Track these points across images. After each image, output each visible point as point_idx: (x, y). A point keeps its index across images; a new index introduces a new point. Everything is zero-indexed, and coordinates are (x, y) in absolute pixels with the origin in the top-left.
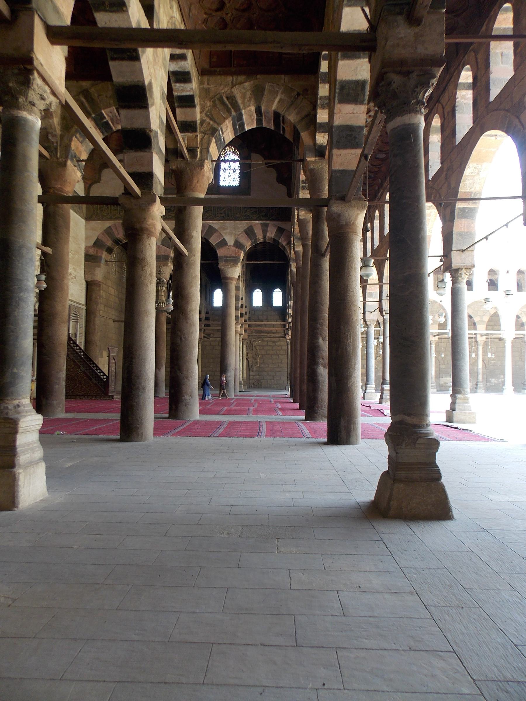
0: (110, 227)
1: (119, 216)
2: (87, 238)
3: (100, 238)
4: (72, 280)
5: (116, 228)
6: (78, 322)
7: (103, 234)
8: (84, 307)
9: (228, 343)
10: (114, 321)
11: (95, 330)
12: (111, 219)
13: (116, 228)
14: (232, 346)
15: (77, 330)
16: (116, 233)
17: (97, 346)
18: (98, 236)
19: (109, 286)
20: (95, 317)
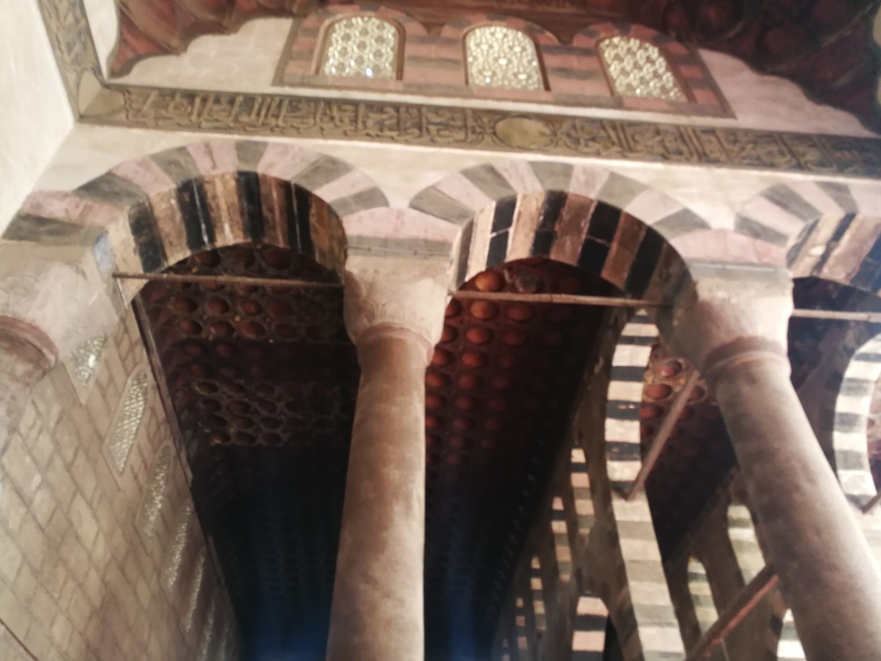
1: (232, 125)
2: (56, 168)
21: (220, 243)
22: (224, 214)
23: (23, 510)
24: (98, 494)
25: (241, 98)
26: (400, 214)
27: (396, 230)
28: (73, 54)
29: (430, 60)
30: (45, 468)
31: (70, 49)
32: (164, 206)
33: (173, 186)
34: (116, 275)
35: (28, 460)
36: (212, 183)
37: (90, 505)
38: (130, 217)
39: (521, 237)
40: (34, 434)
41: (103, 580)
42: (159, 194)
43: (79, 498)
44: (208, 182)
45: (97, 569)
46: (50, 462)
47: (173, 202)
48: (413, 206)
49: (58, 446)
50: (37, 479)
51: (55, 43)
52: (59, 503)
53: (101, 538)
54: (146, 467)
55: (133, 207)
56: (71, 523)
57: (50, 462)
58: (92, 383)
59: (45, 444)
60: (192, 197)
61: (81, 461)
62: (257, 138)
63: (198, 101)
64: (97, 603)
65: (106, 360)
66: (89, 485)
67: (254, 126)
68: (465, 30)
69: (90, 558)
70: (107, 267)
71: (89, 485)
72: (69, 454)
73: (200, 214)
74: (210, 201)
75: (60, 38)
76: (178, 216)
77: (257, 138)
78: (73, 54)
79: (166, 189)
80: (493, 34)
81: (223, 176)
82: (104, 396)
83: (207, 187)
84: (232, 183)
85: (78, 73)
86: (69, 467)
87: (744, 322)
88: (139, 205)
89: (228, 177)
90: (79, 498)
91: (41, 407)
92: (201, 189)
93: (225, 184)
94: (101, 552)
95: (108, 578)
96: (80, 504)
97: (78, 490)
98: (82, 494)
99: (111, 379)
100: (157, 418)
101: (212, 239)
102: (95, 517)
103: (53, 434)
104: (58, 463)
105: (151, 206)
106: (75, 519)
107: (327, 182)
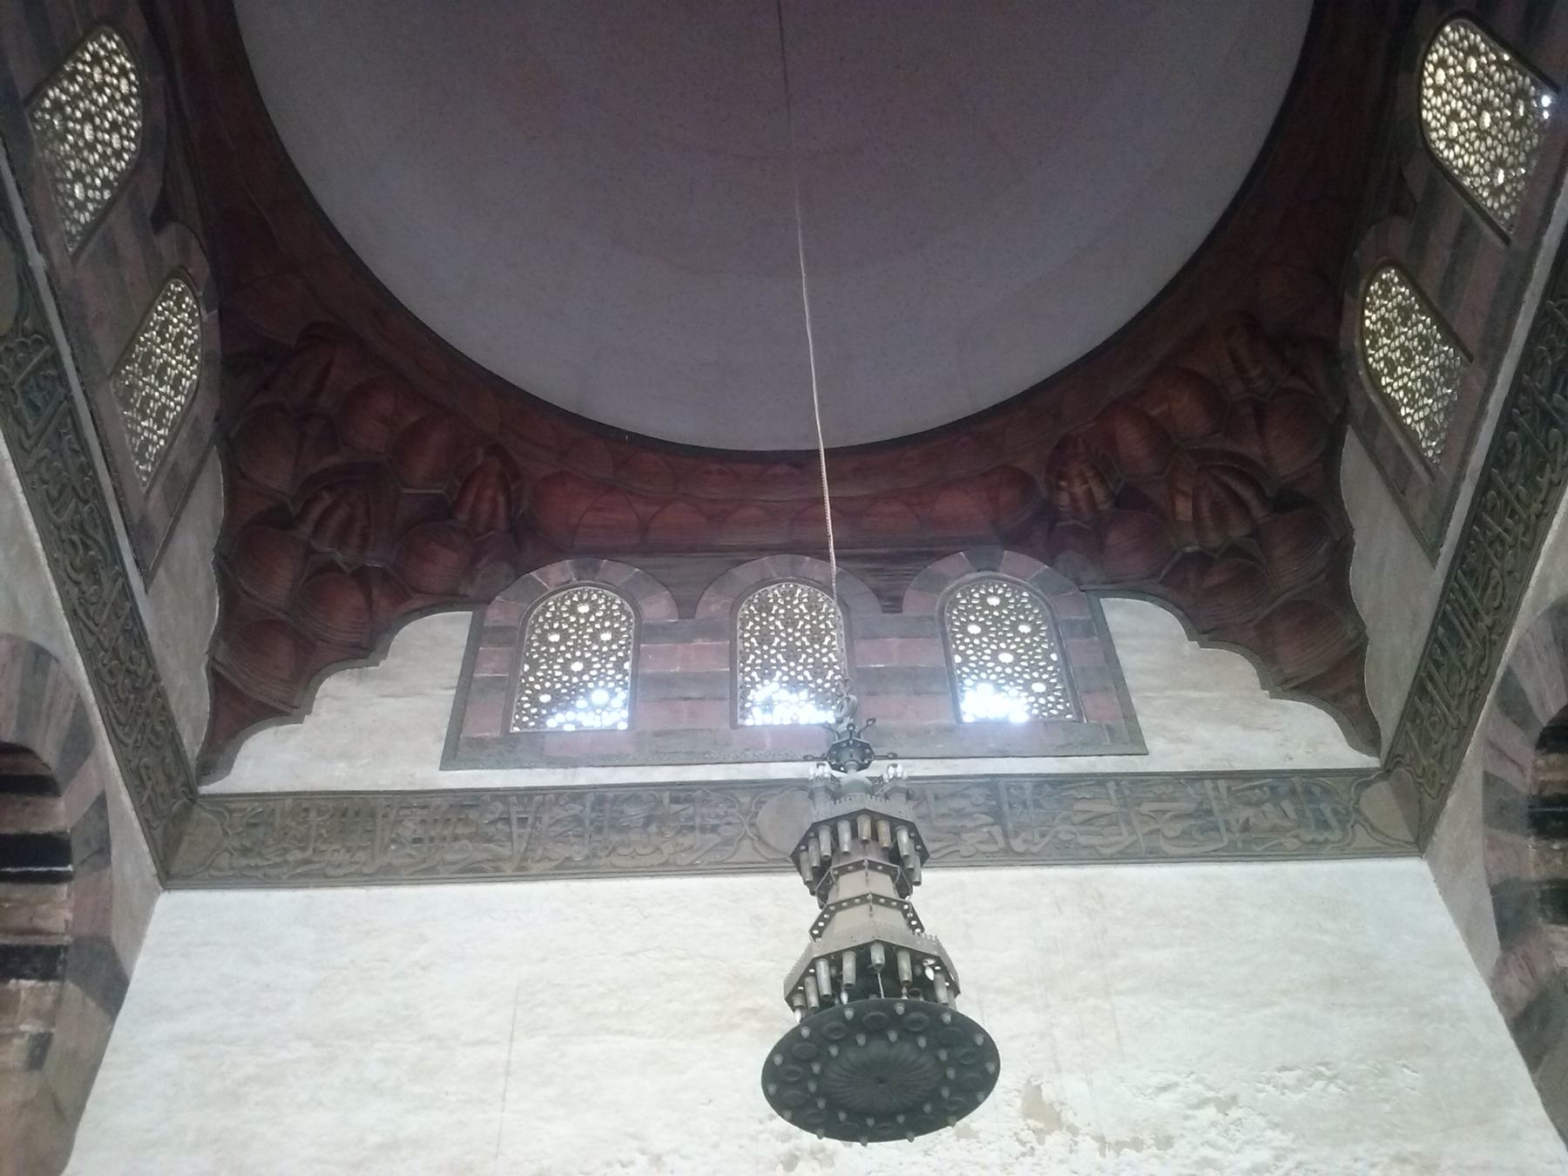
3: (1496, 881)
18: (1489, 875)
25: (1441, 630)
28: (1333, 822)
29: (1451, 272)
31: (1324, 825)
32: (1558, 861)
33: (1532, 839)
36: (1544, 784)
38: (1554, 922)
42: (1537, 865)
44: (1540, 791)
47: (1556, 846)
51: (1311, 851)
55: (1542, 911)
60: (1556, 816)
62: (1500, 672)
63: (1430, 687)
67: (1482, 659)
68: (1420, 145)
75: (1309, 838)
77: (1500, 672)
78: (1333, 822)
79: (1532, 853)
80: (1438, 90)
81: (1536, 769)
83: (1547, 793)
84: (1553, 758)
85: (1356, 821)
88: (1542, 901)
89: (1540, 762)
92: (1547, 802)
93: (1551, 768)
105: (1550, 882)
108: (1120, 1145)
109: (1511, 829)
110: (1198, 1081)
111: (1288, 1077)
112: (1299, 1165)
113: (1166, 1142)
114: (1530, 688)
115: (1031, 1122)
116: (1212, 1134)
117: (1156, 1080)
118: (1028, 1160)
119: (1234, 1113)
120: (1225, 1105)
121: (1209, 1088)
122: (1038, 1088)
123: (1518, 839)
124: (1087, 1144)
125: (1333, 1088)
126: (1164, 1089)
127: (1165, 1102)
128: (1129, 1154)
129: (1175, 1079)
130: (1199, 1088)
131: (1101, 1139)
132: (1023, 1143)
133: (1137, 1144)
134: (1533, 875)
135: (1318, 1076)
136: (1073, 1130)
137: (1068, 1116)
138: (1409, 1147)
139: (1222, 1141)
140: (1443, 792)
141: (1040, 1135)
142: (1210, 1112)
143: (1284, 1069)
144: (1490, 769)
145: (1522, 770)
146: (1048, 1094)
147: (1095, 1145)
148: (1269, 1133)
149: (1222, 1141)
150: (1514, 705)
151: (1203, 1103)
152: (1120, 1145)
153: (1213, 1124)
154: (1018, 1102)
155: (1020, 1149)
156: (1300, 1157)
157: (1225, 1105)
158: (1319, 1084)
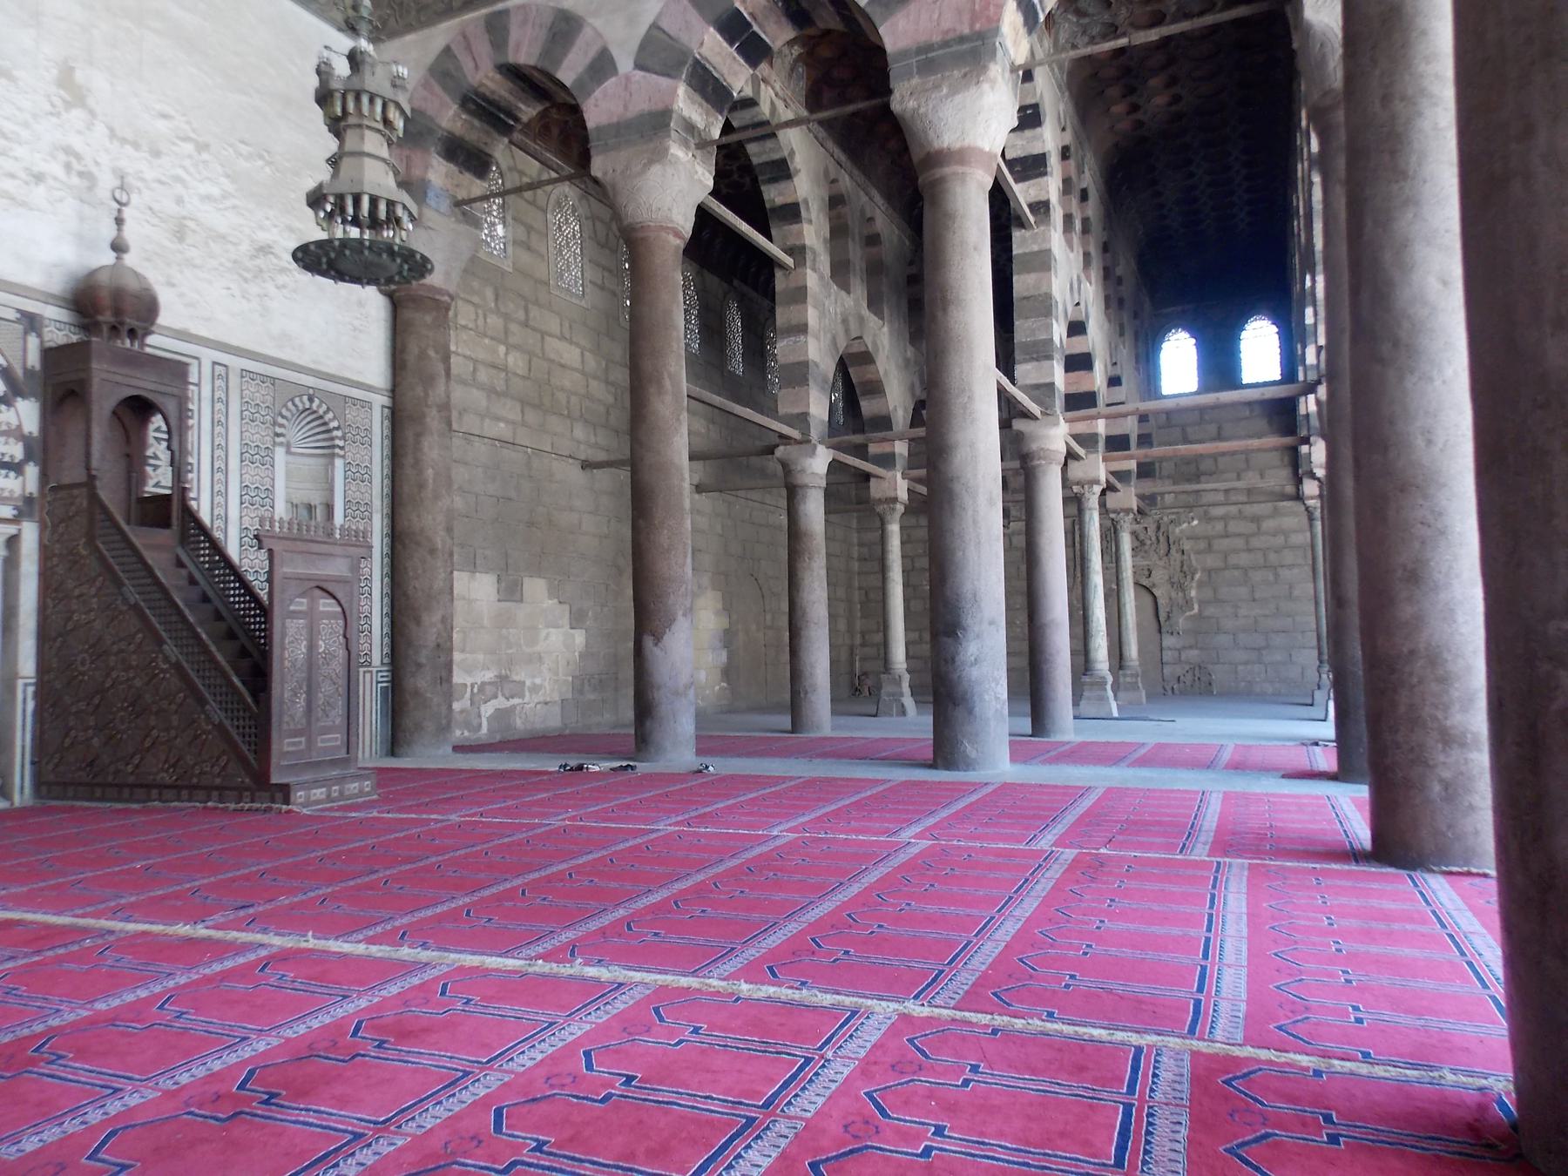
0: (447, 50)
4: (282, 279)
5: (469, 48)
6: (333, 455)
7: (425, 85)
8: (380, 401)
9: (957, 487)
10: (587, 465)
11: (421, 486)
12: (449, 12)
13: (469, 48)
14: (982, 500)
15: (331, 490)
16: (467, 65)
17: (432, 551)
19: (543, 334)
20: (418, 435)
21: (525, 119)
22: (511, 99)
23: (503, 375)
24: (567, 325)
26: (628, 78)
27: (626, 107)
30: (504, 338)
32: (459, 124)
33: (455, 107)
34: (458, 204)
35: (487, 341)
36: (482, 85)
37: (562, 338)
39: (772, 27)
40: (481, 322)
41: (607, 382)
43: (548, 339)
45: (595, 378)
46: (506, 332)
48: (639, 66)
49: (507, 317)
50: (502, 349)
52: (531, 354)
53: (587, 354)
54: (610, 271)
56: (552, 361)
57: (506, 332)
58: (510, 249)
59: (494, 321)
60: (475, 102)
61: (534, 312)
64: (611, 399)
65: (514, 219)
66: (553, 325)
69: (583, 373)
70: (445, 205)
71: (553, 325)
72: (521, 315)
73: (492, 109)
74: (491, 97)
76: (476, 123)
79: (451, 113)
82: (529, 248)
83: (482, 90)
84: (498, 76)
86: (526, 324)
87: (931, 134)
90: (548, 339)
91: (476, 299)
92: (477, 94)
93: (492, 80)
94: (592, 363)
95: (612, 378)
96: (553, 344)
97: (544, 334)
98: (551, 335)
99: (529, 229)
100: (602, 221)
101: (517, 120)
102: (571, 343)
103: (497, 311)
104: (514, 327)
106: (552, 356)
107: (565, 55)
108: (124, 141)
109: (445, 89)
110: (188, 123)
111: (244, 149)
112: (234, 207)
113: (157, 154)
114: (515, 34)
115: (62, 93)
116: (187, 163)
117: (158, 107)
118: (54, 120)
119: (205, 156)
120: (202, 147)
121: (194, 131)
122: (72, 69)
123: (447, 99)
124: (100, 129)
125: (267, 169)
126: (165, 116)
127: (161, 125)
128: (129, 149)
129: (173, 113)
130: (187, 127)
131: (112, 130)
132: (53, 105)
133: (136, 146)
134: (444, 124)
135: (261, 157)
136: (92, 113)
137: (91, 101)
138: (297, 225)
139: (192, 170)
140: (410, 28)
141: (68, 105)
142: (189, 148)
143: (242, 142)
144: (453, 47)
145: (477, 67)
146: (79, 76)
147: (106, 131)
148: (223, 180)
149: (192, 170)
150: (497, 27)
151: (186, 139)
152: (124, 141)
153: (190, 156)
154: (55, 72)
155: (48, 107)
156: (237, 202)
157: (202, 147)
158: (260, 163)
